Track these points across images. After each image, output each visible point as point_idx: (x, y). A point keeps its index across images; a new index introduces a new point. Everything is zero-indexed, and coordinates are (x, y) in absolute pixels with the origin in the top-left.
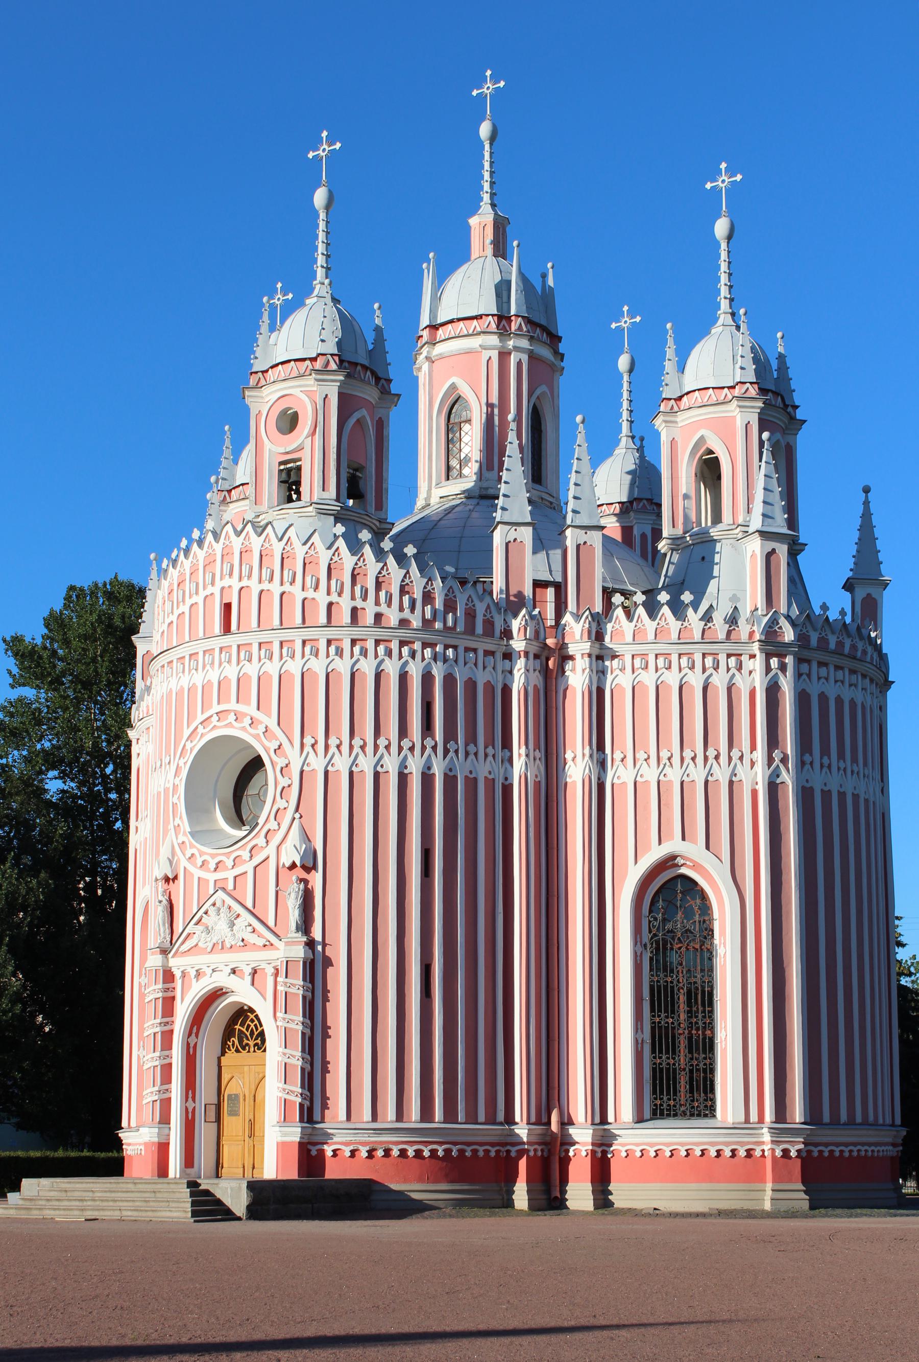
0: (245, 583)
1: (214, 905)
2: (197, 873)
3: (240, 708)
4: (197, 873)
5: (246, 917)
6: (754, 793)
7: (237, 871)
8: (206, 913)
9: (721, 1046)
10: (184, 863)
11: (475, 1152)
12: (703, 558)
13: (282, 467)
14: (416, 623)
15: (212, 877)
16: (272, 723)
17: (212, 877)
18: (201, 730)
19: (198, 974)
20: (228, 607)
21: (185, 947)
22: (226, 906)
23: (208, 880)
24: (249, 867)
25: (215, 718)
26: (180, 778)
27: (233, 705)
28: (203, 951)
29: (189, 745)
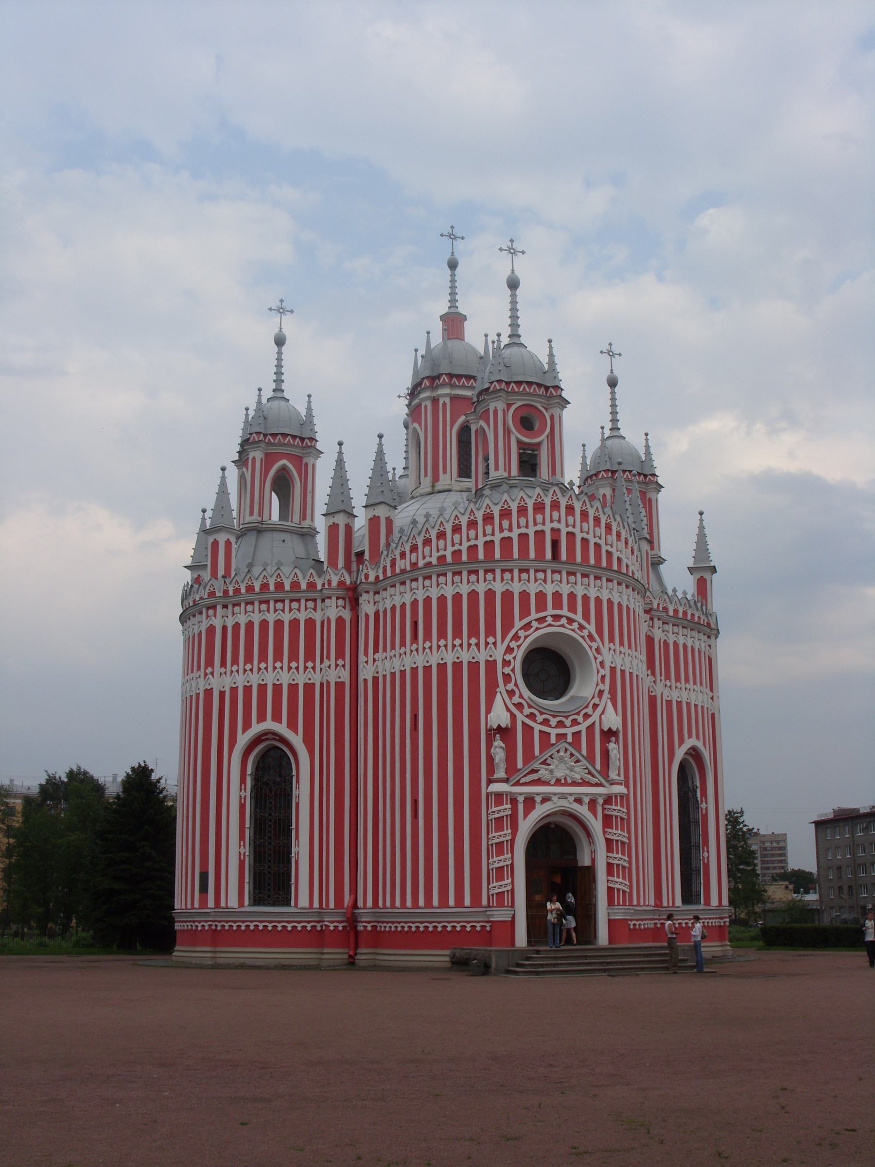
0: (570, 529)
2: (537, 728)
5: (584, 762)
6: (713, 715)
7: (576, 729)
8: (551, 756)
9: (704, 862)
10: (520, 718)
11: (473, 927)
13: (521, 451)
16: (592, 628)
17: (554, 732)
18: (535, 624)
19: (546, 799)
20: (555, 544)
21: (528, 779)
22: (568, 753)
23: (550, 734)
24: (582, 727)
25: (549, 620)
26: (513, 655)
27: (565, 612)
28: (547, 783)
29: (522, 633)
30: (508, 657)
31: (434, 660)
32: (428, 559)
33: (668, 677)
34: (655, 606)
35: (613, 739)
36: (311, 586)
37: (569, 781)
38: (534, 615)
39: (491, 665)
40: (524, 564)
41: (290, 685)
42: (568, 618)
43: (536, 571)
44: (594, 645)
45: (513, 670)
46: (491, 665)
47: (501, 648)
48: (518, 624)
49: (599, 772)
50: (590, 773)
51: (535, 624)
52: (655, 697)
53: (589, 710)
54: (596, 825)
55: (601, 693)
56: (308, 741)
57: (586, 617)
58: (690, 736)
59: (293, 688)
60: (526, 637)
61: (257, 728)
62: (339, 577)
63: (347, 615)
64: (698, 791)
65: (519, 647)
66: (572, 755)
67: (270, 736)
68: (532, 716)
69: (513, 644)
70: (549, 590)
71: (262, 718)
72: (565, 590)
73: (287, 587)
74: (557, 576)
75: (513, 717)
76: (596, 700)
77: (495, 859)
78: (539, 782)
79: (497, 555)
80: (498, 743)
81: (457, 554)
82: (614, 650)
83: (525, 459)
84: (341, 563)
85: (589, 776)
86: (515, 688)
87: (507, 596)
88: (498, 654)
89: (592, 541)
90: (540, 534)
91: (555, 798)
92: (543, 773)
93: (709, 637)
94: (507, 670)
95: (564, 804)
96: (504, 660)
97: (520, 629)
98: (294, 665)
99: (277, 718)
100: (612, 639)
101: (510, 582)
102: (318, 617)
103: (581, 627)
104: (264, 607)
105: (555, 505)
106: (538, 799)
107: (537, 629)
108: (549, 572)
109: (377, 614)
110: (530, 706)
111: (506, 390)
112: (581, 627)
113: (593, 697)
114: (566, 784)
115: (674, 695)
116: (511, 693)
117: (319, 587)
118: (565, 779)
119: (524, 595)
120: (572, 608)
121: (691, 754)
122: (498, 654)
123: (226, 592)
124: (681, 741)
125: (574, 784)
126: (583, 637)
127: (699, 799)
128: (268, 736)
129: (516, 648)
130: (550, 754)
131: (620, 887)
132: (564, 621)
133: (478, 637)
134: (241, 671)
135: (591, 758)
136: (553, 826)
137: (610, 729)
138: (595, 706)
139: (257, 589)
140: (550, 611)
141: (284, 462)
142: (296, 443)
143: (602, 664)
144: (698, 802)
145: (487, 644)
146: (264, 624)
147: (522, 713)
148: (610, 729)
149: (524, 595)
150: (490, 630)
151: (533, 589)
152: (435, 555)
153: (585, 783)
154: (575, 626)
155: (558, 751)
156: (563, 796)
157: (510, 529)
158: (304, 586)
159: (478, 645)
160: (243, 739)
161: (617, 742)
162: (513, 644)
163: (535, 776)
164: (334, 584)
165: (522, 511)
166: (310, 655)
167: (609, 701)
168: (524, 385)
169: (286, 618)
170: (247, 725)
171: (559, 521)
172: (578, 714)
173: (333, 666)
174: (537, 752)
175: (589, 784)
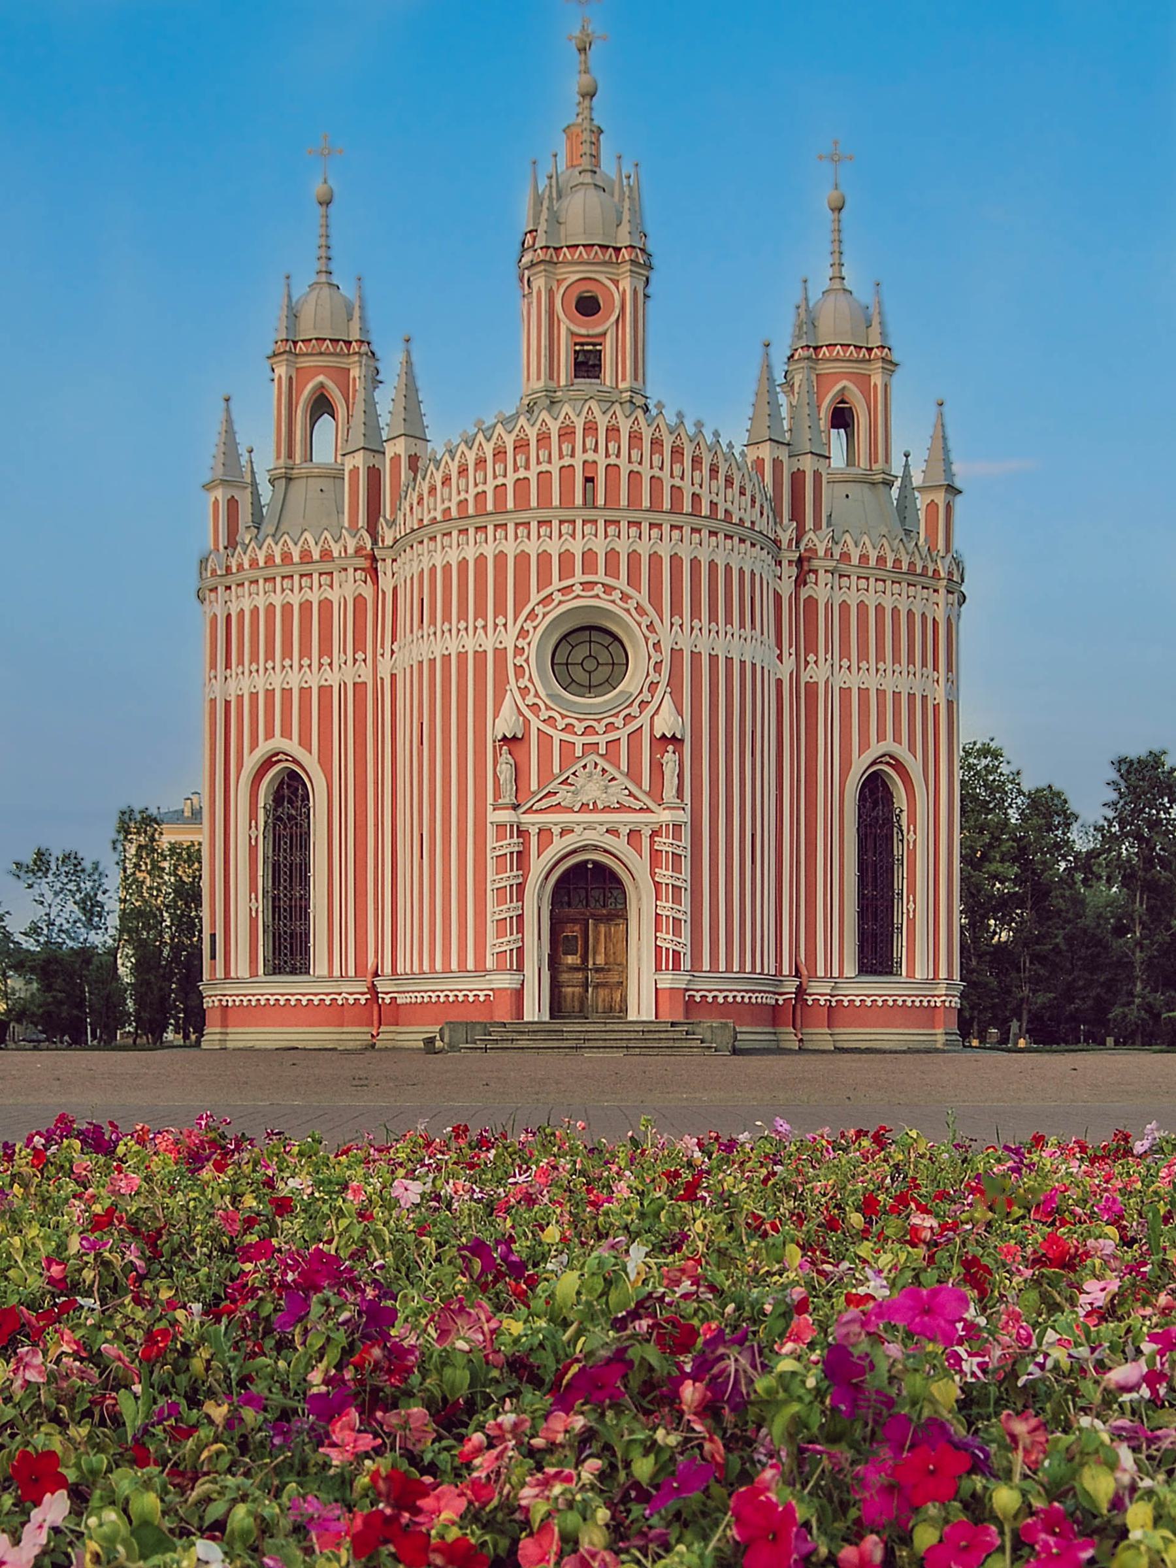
0: (613, 460)
1: (585, 767)
2: (557, 736)
3: (609, 581)
4: (557, 736)
5: (621, 779)
6: (936, 707)
8: (574, 774)
10: (535, 724)
12: (847, 496)
13: (578, 348)
14: (748, 524)
15: (579, 741)
16: (643, 598)
17: (579, 741)
18: (558, 597)
21: (544, 804)
22: (599, 768)
24: (623, 734)
25: (578, 589)
26: (528, 640)
27: (601, 577)
28: (570, 810)
29: (540, 610)
30: (521, 643)
31: (470, 645)
32: (433, 514)
33: (845, 653)
34: (821, 553)
35: (670, 748)
36: (326, 555)
37: (600, 806)
38: (556, 584)
39: (500, 654)
40: (544, 514)
41: (301, 689)
42: (603, 585)
43: (561, 522)
44: (645, 621)
45: (527, 661)
46: (500, 654)
47: (513, 631)
48: (535, 597)
49: (648, 794)
50: (631, 794)
51: (558, 597)
52: (817, 683)
53: (634, 710)
54: (640, 864)
55: (653, 686)
56: (325, 761)
57: (633, 581)
58: (881, 737)
59: (305, 692)
60: (544, 615)
61: (265, 748)
62: (356, 540)
63: (367, 591)
64: (904, 815)
65: (535, 628)
66: (604, 770)
67: (281, 757)
68: (550, 721)
69: (528, 626)
70: (577, 548)
71: (269, 735)
72: (600, 546)
73: (296, 559)
74: (588, 528)
75: (527, 722)
76: (646, 696)
77: (496, 909)
78: (557, 808)
79: (510, 505)
80: (505, 756)
81: (463, 504)
82: (681, 626)
83: (581, 358)
84: (362, 521)
85: (632, 799)
86: (530, 686)
87: (522, 559)
88: (509, 640)
89: (647, 474)
90: (567, 471)
91: (578, 829)
92: (564, 796)
93: (936, 591)
94: (520, 661)
95: (592, 837)
96: (516, 646)
97: (538, 604)
98: (306, 662)
99: (286, 733)
100: (676, 609)
101: (526, 540)
102: (334, 595)
103: (625, 597)
104: (269, 586)
105: (590, 428)
106: (556, 830)
107: (560, 602)
108: (579, 523)
109: (395, 589)
110: (548, 708)
111: (555, 260)
112: (625, 597)
113: (641, 692)
114: (595, 809)
115: (853, 681)
116: (524, 691)
117: (336, 554)
118: (595, 803)
119: (544, 557)
120: (612, 569)
121: (888, 763)
122: (509, 640)
123: (228, 568)
124: (864, 746)
125: (607, 809)
126: (628, 611)
127: (905, 828)
128: (281, 757)
129: (531, 630)
130: (572, 771)
131: (668, 946)
132: (599, 589)
133: (485, 619)
134: (247, 673)
135: (633, 774)
136: (590, 866)
137: (664, 735)
138: (643, 704)
139: (261, 564)
140: (579, 577)
141: (321, 378)
142: (338, 350)
143: (657, 645)
144: (902, 831)
145: (496, 625)
146: (271, 608)
147: (538, 717)
148: (664, 735)
149: (544, 557)
150: (500, 610)
151: (554, 548)
152: (440, 507)
153: (622, 808)
154: (616, 595)
155: (585, 767)
156: (589, 827)
157: (527, 468)
158: (316, 556)
159: (485, 627)
160: (252, 761)
161: (679, 751)
162: (528, 626)
163: (554, 801)
164: (351, 551)
165: (544, 438)
166: (326, 649)
167: (667, 696)
168: (581, 248)
169: (295, 600)
170: (254, 745)
171: (596, 450)
172: (616, 715)
173: (350, 662)
174: (556, 770)
175: (631, 809)
